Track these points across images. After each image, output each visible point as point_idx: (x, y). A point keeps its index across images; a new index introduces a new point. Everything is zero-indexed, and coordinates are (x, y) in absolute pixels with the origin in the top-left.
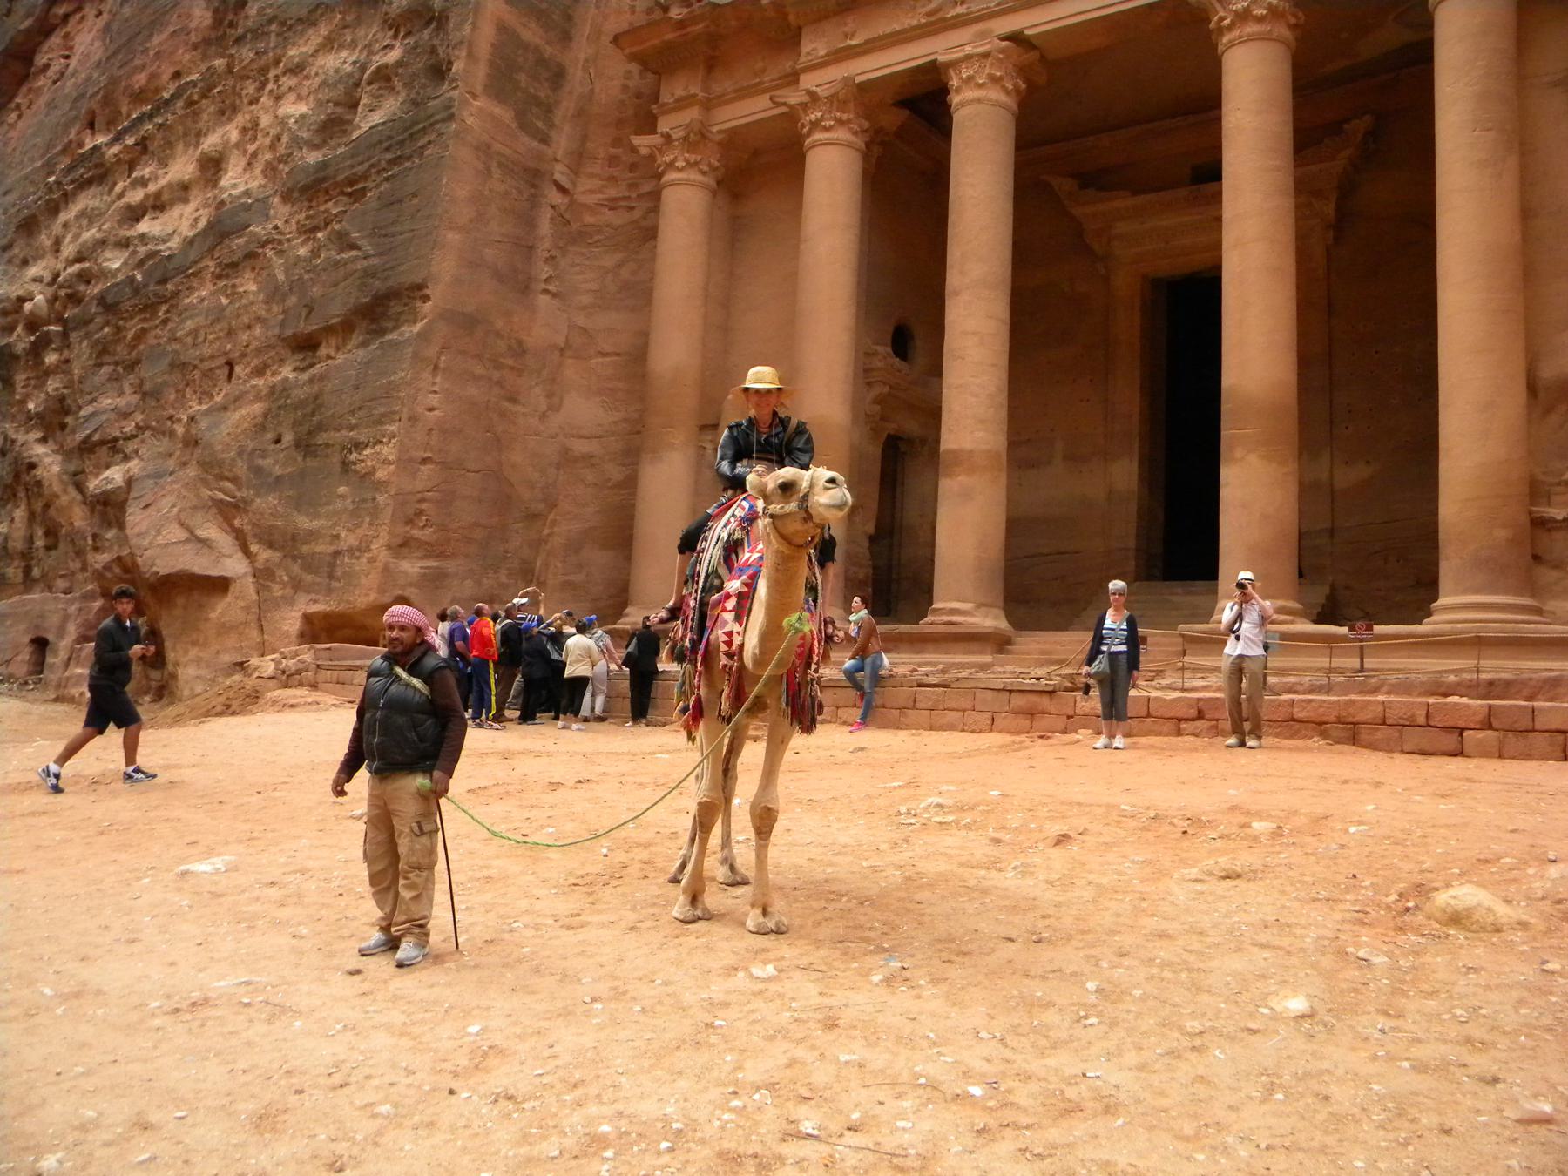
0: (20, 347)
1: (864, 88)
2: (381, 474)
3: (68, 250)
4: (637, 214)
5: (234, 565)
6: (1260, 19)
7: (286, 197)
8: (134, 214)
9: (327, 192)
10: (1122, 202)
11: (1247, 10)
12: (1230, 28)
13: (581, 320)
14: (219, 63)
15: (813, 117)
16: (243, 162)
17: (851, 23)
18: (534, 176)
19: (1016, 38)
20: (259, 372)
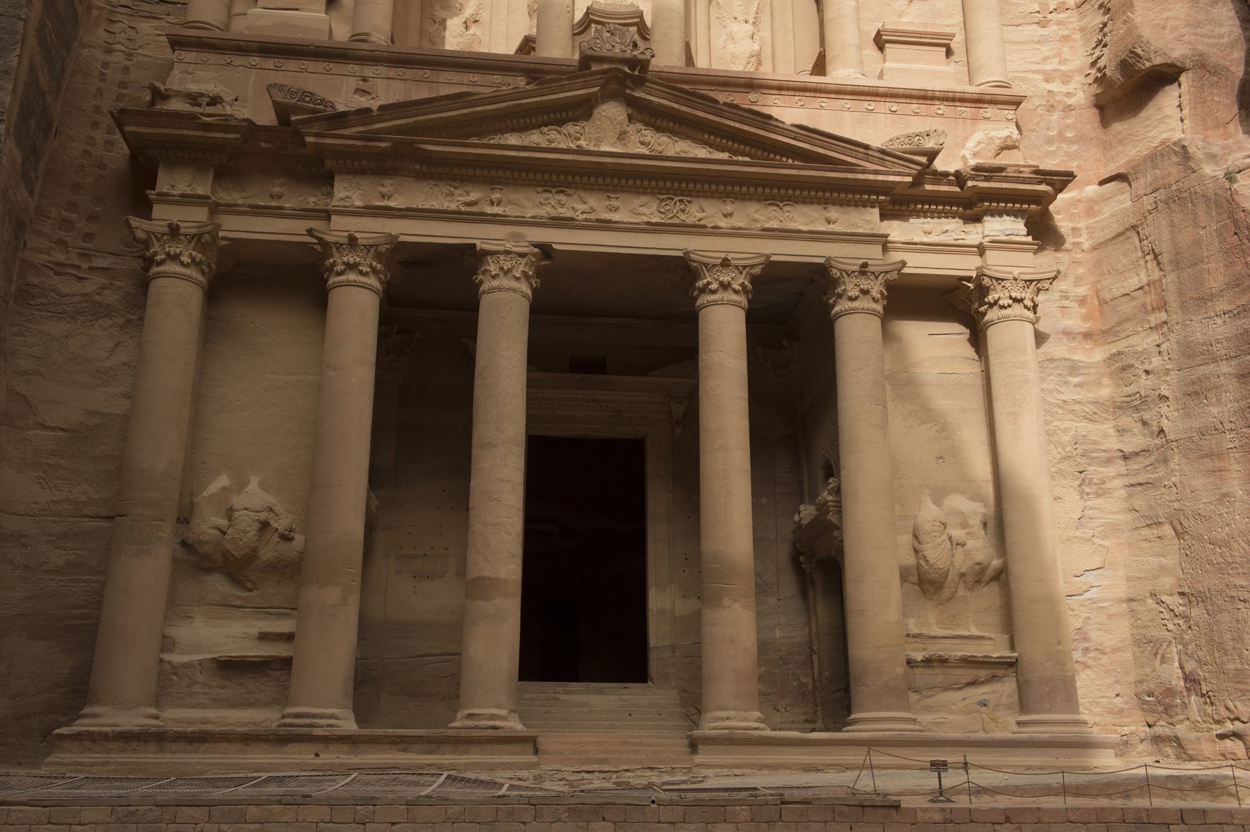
4: (89, 287)
6: (736, 292)
11: (729, 284)
12: (714, 292)
15: (351, 260)
17: (388, 185)
19: (546, 250)
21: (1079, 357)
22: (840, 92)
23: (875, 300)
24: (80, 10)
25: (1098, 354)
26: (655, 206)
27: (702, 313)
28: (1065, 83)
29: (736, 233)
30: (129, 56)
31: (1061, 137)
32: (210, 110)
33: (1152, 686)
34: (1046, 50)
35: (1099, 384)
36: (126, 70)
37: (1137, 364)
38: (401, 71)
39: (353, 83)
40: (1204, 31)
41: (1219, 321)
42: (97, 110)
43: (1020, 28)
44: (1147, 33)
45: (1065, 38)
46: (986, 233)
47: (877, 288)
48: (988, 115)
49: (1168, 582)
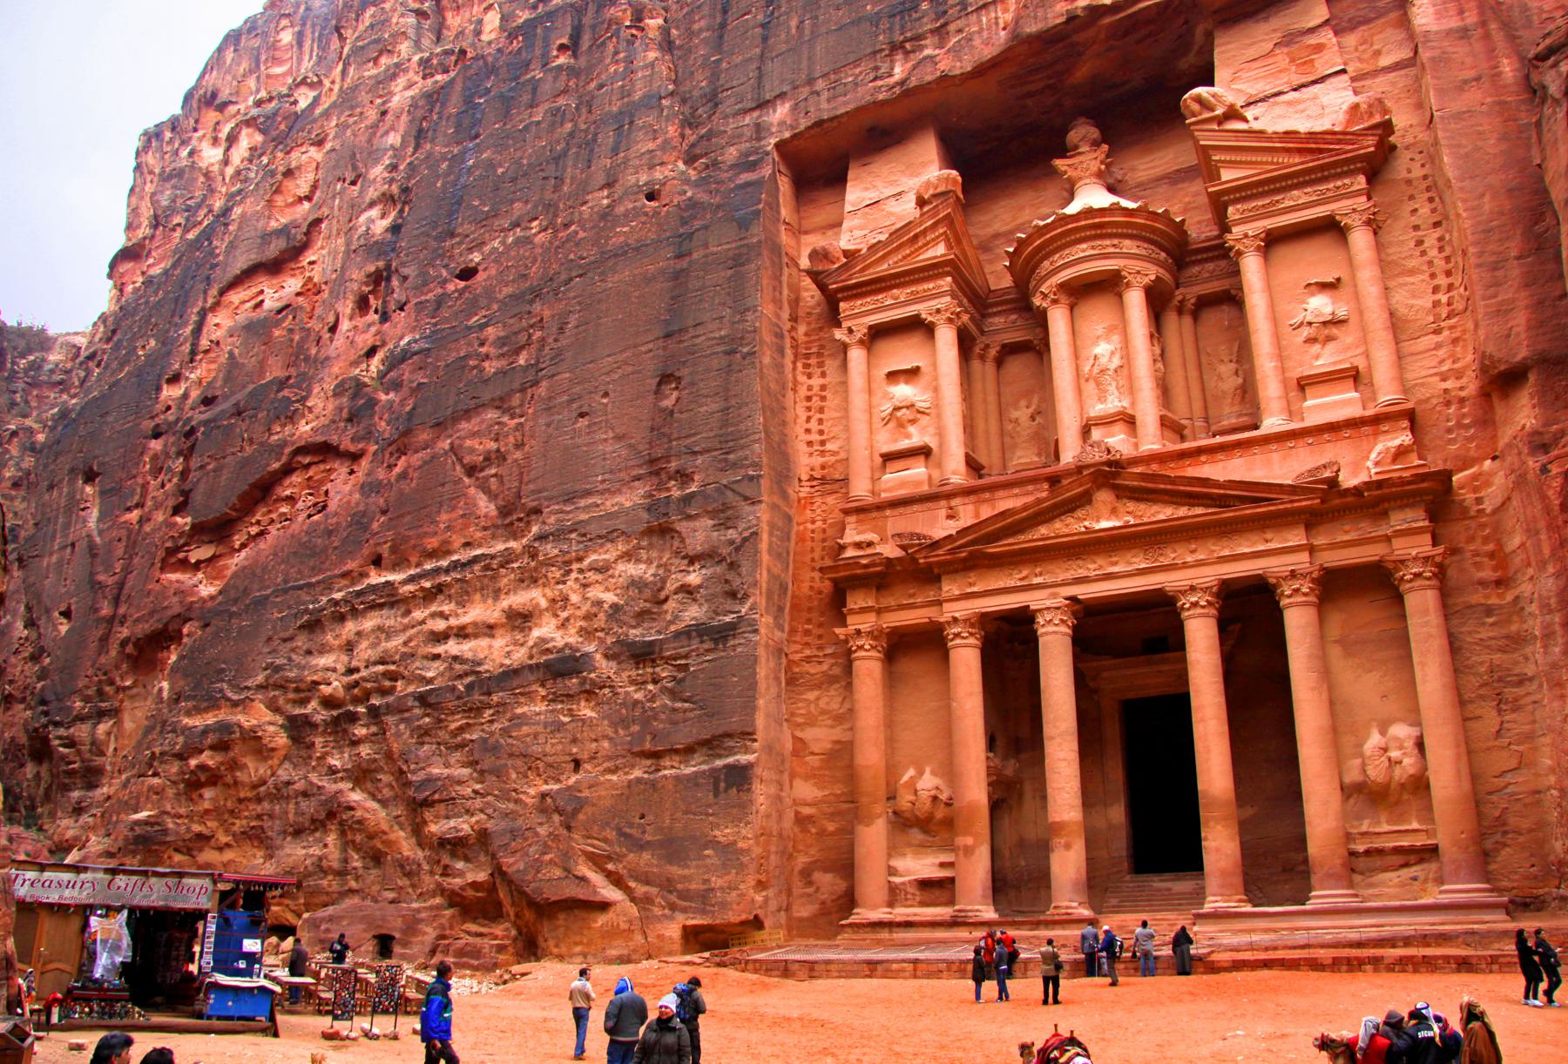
0: (318, 718)
1: (984, 615)
2: (740, 845)
3: (364, 651)
4: (825, 667)
5: (610, 893)
7: (606, 656)
8: (441, 637)
9: (653, 661)
10: (1107, 662)
13: (799, 734)
14: (512, 544)
15: (955, 630)
16: (554, 622)
17: (972, 577)
18: (779, 651)
19: (1073, 599)
20: (614, 771)
21: (1493, 601)
23: (1305, 594)
24: (792, 512)
25: (1509, 597)
30: (824, 521)
32: (869, 551)
33: (1552, 858)
34: (1442, 353)
35: (1509, 621)
36: (824, 531)
38: (973, 498)
39: (943, 512)
42: (813, 560)
44: (1490, 349)
45: (1455, 341)
49: (1552, 779)
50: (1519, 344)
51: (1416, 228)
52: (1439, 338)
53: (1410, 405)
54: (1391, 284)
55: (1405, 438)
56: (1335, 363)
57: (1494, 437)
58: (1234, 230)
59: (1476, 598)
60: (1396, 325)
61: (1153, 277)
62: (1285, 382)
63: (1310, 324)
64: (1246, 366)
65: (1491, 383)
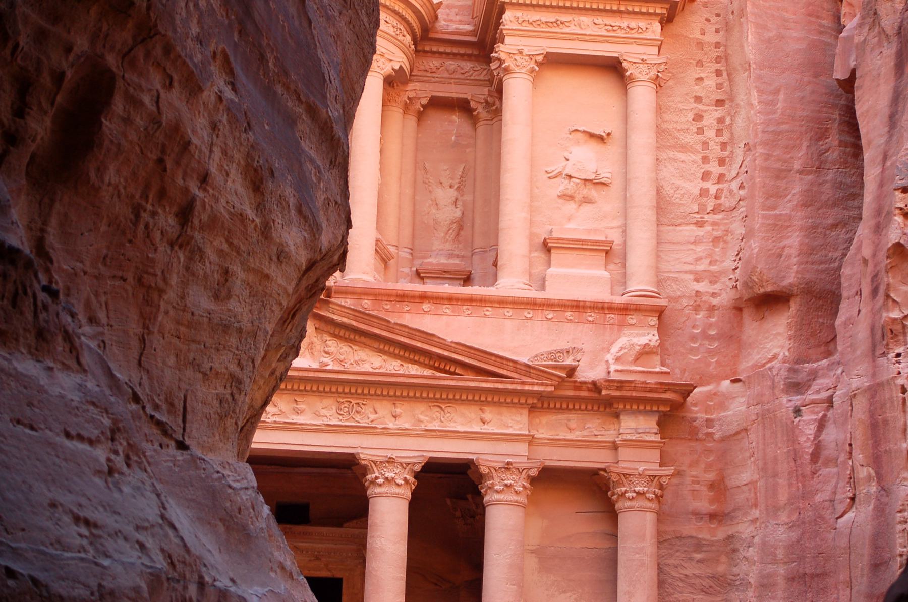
12: (380, 485)
21: (704, 535)
22: (502, 302)
25: (721, 535)
26: (334, 408)
27: (371, 500)
28: (716, 282)
29: (402, 433)
31: (705, 335)
34: (699, 249)
35: (717, 561)
37: (741, 549)
40: (816, 257)
41: (782, 529)
43: (678, 228)
45: (716, 240)
46: (621, 431)
47: (520, 483)
48: (634, 321)
50: (788, 267)
51: (698, 99)
52: (700, 232)
53: (662, 302)
54: (663, 156)
55: (649, 337)
56: (589, 231)
57: (736, 356)
58: (508, 40)
59: (689, 529)
60: (662, 206)
61: (397, 67)
62: (532, 236)
63: (570, 177)
64: (468, 197)
65: (749, 300)
